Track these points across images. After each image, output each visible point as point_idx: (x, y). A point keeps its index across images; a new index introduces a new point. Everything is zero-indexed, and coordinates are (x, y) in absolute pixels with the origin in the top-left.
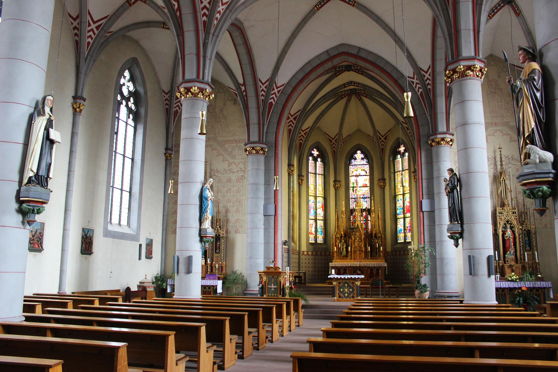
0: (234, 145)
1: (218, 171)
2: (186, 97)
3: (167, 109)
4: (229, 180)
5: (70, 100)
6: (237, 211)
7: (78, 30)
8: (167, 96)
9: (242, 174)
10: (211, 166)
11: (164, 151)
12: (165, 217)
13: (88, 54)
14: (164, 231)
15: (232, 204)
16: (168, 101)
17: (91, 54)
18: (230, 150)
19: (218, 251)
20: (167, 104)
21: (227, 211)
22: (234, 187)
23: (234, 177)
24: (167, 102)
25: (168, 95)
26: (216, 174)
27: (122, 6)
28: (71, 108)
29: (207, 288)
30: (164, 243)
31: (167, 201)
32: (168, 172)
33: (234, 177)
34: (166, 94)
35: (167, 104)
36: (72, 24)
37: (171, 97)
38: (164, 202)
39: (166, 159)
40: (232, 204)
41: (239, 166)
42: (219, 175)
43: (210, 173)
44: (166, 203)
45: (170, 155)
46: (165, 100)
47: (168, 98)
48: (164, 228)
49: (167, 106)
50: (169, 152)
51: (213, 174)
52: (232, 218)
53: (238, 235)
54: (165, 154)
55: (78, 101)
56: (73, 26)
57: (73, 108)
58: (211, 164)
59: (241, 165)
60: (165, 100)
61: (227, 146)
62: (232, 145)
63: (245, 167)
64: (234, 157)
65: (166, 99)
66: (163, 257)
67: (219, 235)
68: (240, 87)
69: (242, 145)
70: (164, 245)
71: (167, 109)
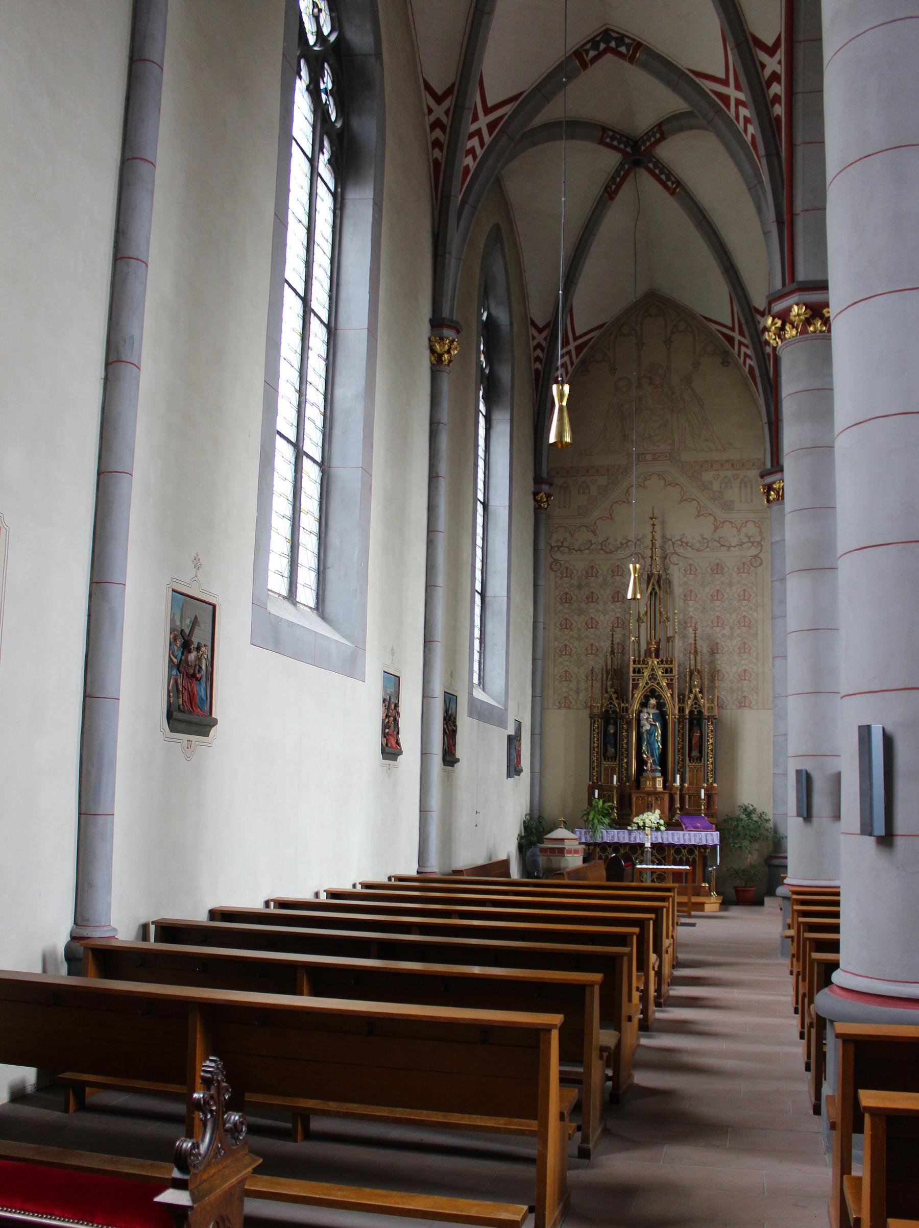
0: (730, 473)
1: (684, 544)
2: (804, 332)
3: (537, 372)
4: (718, 568)
5: (425, 329)
6: (744, 649)
7: (444, 133)
8: (540, 338)
9: (754, 551)
10: (663, 529)
11: (531, 487)
12: (539, 663)
13: (464, 202)
14: (538, 699)
15: (727, 631)
16: (542, 349)
17: (471, 200)
18: (716, 486)
19: (695, 753)
20: (537, 359)
21: (713, 651)
22: (730, 585)
23: (731, 559)
24: (539, 352)
25: (545, 334)
26: (681, 551)
27: (560, 68)
28: (427, 353)
29: (684, 852)
30: (537, 731)
31: (541, 619)
32: (542, 544)
33: (731, 559)
34: (540, 331)
35: (537, 359)
36: (430, 111)
37: (553, 337)
38: (535, 623)
39: (538, 509)
40: (727, 631)
41: (744, 531)
42: (689, 553)
43: (662, 548)
44: (541, 626)
45: (548, 496)
46: (535, 348)
47: (544, 344)
48: (538, 692)
49: (538, 365)
50: (545, 488)
51: (670, 550)
52: (729, 667)
53: (747, 712)
54: (535, 494)
55: (447, 332)
56: (433, 118)
57: (432, 351)
58: (663, 523)
59: (751, 529)
60: (535, 348)
61: (707, 476)
62: (723, 473)
63: (761, 532)
64: (728, 506)
65: (539, 346)
66: (537, 769)
67: (700, 712)
68: (753, 319)
69: (754, 473)
70: (537, 737)
71: (537, 372)
